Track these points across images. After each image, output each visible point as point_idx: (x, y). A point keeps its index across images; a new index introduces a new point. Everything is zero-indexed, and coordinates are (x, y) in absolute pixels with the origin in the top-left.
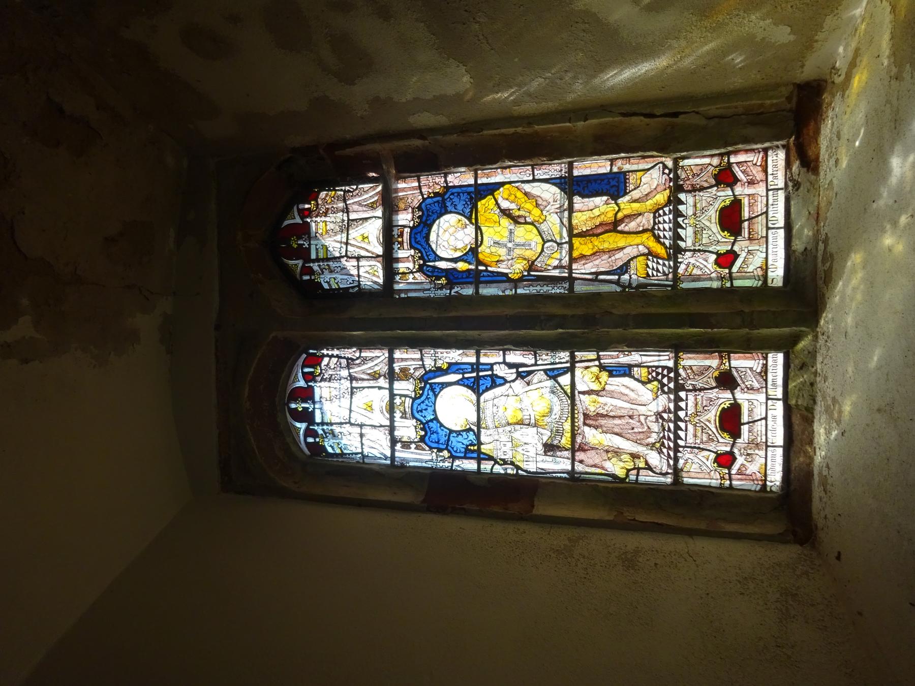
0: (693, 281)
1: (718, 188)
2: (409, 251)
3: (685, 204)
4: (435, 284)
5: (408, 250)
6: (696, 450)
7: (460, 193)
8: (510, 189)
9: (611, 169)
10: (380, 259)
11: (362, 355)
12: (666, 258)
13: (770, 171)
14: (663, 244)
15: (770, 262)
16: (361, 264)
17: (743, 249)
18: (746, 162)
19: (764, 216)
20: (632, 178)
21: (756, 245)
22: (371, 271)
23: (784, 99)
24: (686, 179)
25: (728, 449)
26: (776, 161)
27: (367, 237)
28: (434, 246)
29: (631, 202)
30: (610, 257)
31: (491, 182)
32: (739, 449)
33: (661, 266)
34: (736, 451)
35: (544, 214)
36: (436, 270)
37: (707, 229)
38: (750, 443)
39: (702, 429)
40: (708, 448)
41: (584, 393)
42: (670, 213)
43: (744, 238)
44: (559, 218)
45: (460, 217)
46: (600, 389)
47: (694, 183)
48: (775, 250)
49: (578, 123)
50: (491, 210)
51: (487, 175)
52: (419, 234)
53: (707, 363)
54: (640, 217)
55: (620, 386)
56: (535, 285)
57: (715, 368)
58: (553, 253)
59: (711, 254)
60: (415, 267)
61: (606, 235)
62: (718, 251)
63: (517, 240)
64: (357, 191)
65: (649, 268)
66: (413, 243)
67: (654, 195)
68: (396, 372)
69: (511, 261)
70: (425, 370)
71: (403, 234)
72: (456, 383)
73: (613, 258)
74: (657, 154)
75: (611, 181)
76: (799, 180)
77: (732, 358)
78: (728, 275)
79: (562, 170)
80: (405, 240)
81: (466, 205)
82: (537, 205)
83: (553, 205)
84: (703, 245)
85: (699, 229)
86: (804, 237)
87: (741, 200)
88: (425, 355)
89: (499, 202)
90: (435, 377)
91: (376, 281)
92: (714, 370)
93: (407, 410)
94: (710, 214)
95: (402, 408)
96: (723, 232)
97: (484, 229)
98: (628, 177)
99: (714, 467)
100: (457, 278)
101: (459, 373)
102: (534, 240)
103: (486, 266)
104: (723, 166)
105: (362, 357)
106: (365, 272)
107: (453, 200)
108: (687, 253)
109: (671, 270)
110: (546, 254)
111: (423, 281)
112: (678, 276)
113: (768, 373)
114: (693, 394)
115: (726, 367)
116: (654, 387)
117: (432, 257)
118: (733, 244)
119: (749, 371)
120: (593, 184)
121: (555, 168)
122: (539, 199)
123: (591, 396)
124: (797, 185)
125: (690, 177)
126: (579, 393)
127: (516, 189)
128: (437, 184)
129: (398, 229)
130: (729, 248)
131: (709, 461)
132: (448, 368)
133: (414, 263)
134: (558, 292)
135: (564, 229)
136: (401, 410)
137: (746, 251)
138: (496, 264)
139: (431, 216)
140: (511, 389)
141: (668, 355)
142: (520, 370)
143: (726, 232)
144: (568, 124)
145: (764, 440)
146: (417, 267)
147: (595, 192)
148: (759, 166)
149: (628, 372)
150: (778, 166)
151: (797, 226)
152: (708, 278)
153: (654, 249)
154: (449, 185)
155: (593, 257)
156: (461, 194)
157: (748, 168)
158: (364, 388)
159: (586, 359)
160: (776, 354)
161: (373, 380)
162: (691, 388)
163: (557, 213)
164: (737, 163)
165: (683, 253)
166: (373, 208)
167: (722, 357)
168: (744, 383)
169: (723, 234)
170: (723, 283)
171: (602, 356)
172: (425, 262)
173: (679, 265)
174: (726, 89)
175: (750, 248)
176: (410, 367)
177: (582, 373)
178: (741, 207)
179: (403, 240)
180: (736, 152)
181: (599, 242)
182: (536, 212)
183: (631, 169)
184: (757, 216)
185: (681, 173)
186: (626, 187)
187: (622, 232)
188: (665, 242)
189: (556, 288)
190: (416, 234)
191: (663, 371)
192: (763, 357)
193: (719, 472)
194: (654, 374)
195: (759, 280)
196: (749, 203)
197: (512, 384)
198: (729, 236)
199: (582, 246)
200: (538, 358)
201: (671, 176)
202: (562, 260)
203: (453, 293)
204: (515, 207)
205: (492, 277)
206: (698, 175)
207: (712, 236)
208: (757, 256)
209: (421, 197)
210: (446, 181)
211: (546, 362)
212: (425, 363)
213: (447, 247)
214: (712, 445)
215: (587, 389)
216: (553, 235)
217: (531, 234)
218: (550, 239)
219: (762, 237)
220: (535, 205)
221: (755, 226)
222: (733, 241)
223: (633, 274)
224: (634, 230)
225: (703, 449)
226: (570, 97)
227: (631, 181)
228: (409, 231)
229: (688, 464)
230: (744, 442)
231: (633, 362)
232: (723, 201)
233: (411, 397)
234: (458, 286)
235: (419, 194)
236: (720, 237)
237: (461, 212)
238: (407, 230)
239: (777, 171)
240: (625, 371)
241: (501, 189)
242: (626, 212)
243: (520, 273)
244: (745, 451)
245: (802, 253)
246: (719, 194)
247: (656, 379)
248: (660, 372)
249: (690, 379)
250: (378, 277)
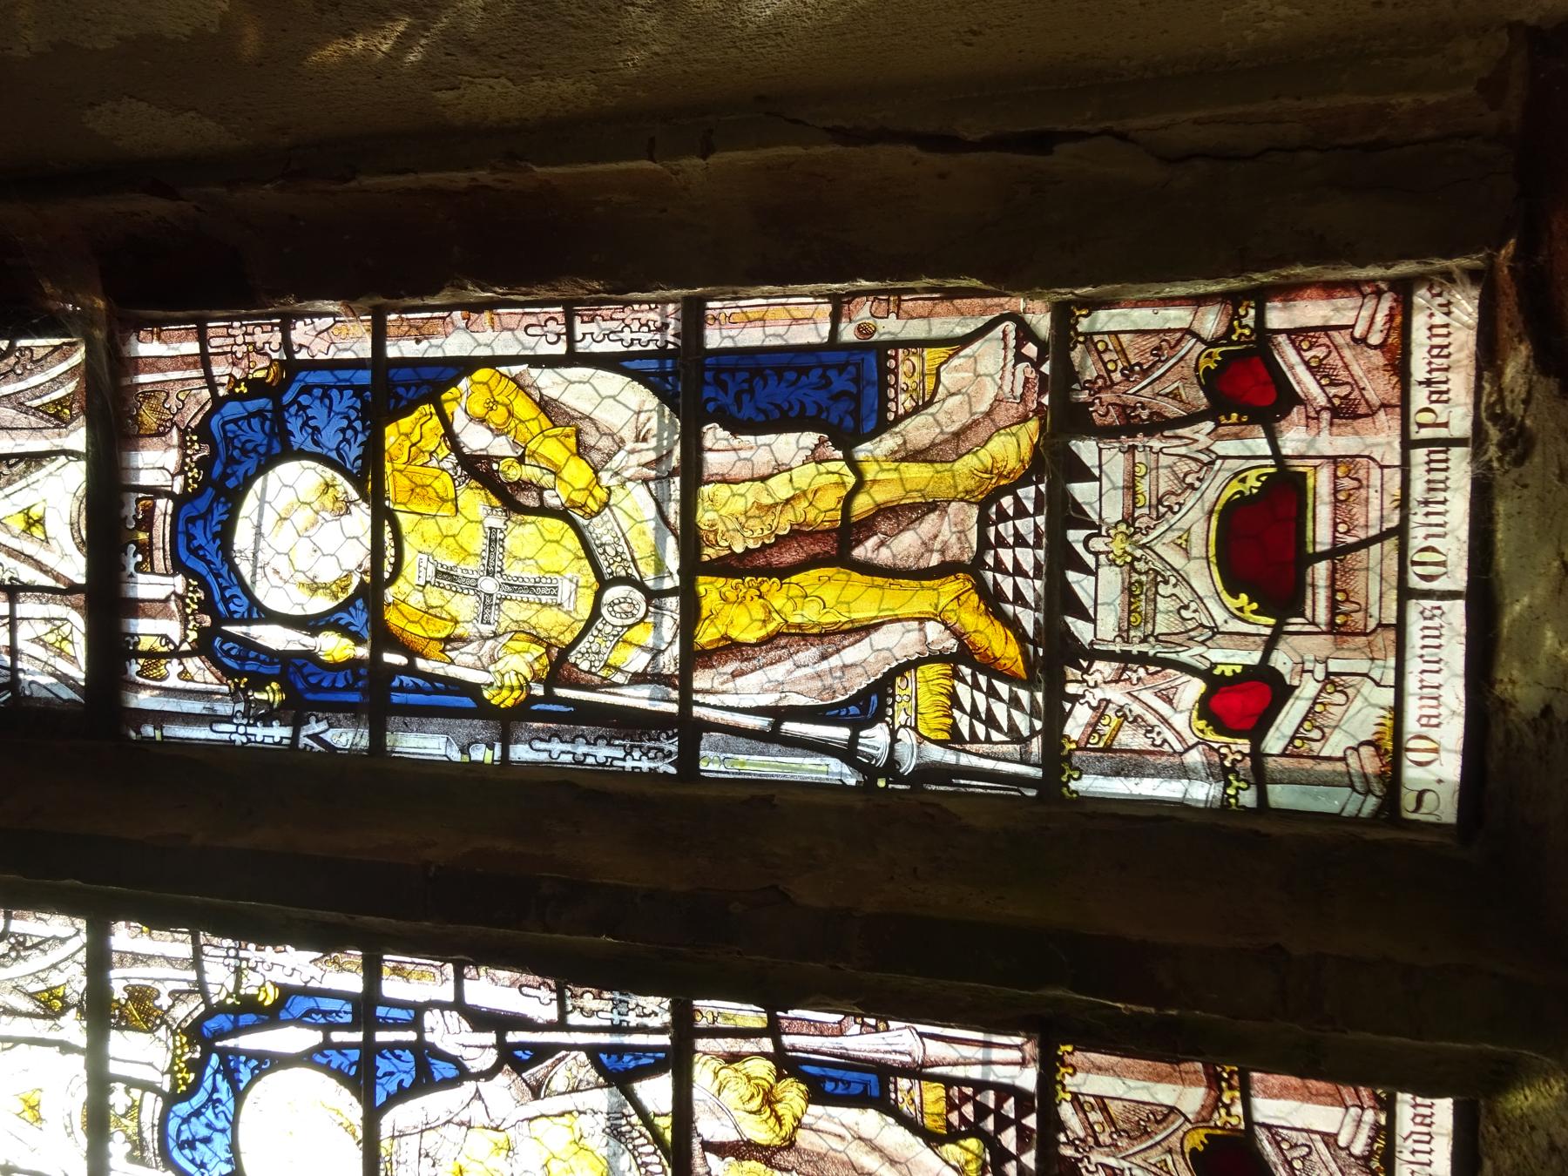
0: (1117, 774)
1: (1218, 424)
2: (169, 580)
3: (1092, 478)
4: (247, 701)
5: (167, 575)
7: (331, 387)
8: (493, 383)
9: (834, 331)
10: (80, 598)
11: (12, 929)
12: (1023, 675)
13: (1419, 370)
14: (1013, 624)
15: (1411, 725)
16: (22, 610)
17: (1308, 666)
18: (1326, 329)
19: (1391, 544)
20: (906, 367)
21: (1357, 654)
22: (51, 638)
23: (1469, 90)
24: (1100, 382)
26: (1444, 331)
27: (40, 521)
28: (245, 569)
29: (903, 460)
30: (824, 657)
31: (431, 354)
33: (1003, 707)
35: (603, 483)
36: (252, 654)
37: (1173, 580)
41: (721, 1149)
42: (1038, 511)
43: (1317, 625)
44: (656, 500)
45: (329, 473)
46: (777, 1142)
47: (1131, 400)
48: (1431, 679)
49: (684, 162)
50: (431, 454)
51: (418, 328)
52: (200, 523)
53: (1165, 1094)
54: (933, 516)
55: (849, 1137)
56: (567, 737)
57: (1190, 1117)
58: (630, 627)
59: (1188, 677)
60: (186, 636)
61: (814, 573)
62: (1214, 665)
63: (513, 570)
64: (12, 360)
65: (962, 709)
66: (184, 554)
67: (985, 435)
68: (116, 997)
69: (490, 643)
70: (206, 1000)
71: (153, 516)
72: (305, 1059)
73: (835, 661)
74: (976, 283)
75: (832, 374)
76: (1528, 422)
77: (1257, 1087)
78: (1248, 760)
79: (665, 326)
80: (158, 542)
81: (349, 433)
82: (582, 450)
83: (632, 452)
84: (1157, 640)
85: (1144, 578)
86: (1542, 659)
87: (1304, 475)
88: (206, 949)
89: (457, 428)
90: (237, 1031)
91: (66, 675)
92: (1190, 1126)
93: (147, 1135)
94: (1184, 524)
95: (132, 1127)
96: (1235, 595)
97: (405, 521)
98: (892, 363)
100: (317, 688)
101: (315, 1026)
102: (568, 574)
103: (411, 652)
104: (1238, 343)
105: (13, 935)
106: (33, 641)
107: (310, 412)
108: (1098, 665)
109: (1038, 725)
110: (608, 629)
111: (210, 687)
112: (1063, 747)
113: (1398, 1162)
115: (1234, 1121)
116: (970, 1156)
117: (240, 607)
118: (1270, 645)
119: (1321, 1146)
120: (772, 382)
121: (644, 317)
122: (586, 426)
123: (746, 1163)
124: (1518, 443)
125: (1117, 376)
126: (708, 1146)
127: (513, 385)
128: (260, 352)
129: (138, 500)
130: (1254, 658)
132: (280, 1004)
133: (185, 621)
134: (645, 769)
135: (671, 544)
136: (130, 1132)
137: (1320, 673)
138: (443, 651)
139: (240, 463)
140: (477, 1104)
141: (1019, 1047)
142: (513, 1037)
143: (1244, 597)
144: (647, 164)
146: (193, 635)
147: (777, 414)
148: (1375, 347)
149: (875, 1092)
150: (1451, 349)
151: (1517, 608)
152: (1172, 766)
153: (979, 640)
154: (298, 356)
155: (767, 652)
156: (335, 393)
157: (1334, 354)
158: (16, 1041)
159: (730, 1024)
160: (1428, 1101)
161: (44, 1017)
163: (645, 481)
164: (1296, 334)
165: (1085, 664)
166: (62, 420)
167: (1219, 1078)
169: (1232, 603)
170: (1231, 791)
171: (785, 1023)
172: (218, 620)
173: (1068, 706)
174: (1229, 45)
175: (1334, 666)
176: (158, 986)
177: (716, 1074)
178: (1306, 505)
179: (151, 537)
180: (1289, 291)
181: (789, 598)
182: (577, 473)
183: (903, 336)
184: (1366, 543)
185: (1083, 359)
186: (884, 400)
187: (868, 569)
188: (1020, 616)
189: (637, 754)
190: (191, 520)
191: (1000, 1102)
192: (1377, 1098)
194: (968, 1110)
195: (1368, 792)
196: (1336, 492)
197: (483, 1085)
198: (1254, 612)
199: (727, 607)
200: (569, 1002)
201: (1046, 368)
202: (660, 652)
203: (304, 741)
204: (507, 451)
205: (428, 693)
206: (1145, 373)
207: (1193, 606)
208: (1359, 698)
209: (206, 394)
210: (286, 344)
211: (593, 1021)
212: (208, 978)
213: (286, 575)
215: (732, 1136)
216: (634, 560)
217: (559, 548)
218: (623, 573)
219: (1380, 625)
220: (575, 451)
221: (1357, 583)
222: (1268, 631)
223: (905, 726)
224: (911, 563)
226: (634, 59)
227: (902, 379)
228: (170, 511)
231: (893, 1056)
232: (1236, 474)
233: (158, 1092)
234: (320, 715)
235: (202, 383)
236: (1220, 615)
237: (334, 455)
238: (164, 505)
239: (1446, 370)
240: (866, 1084)
241: (464, 384)
242: (882, 495)
243: (521, 687)
245: (1534, 724)
246: (1222, 447)
247: (975, 1130)
248: (992, 1105)
249: (1098, 1143)
250: (73, 660)
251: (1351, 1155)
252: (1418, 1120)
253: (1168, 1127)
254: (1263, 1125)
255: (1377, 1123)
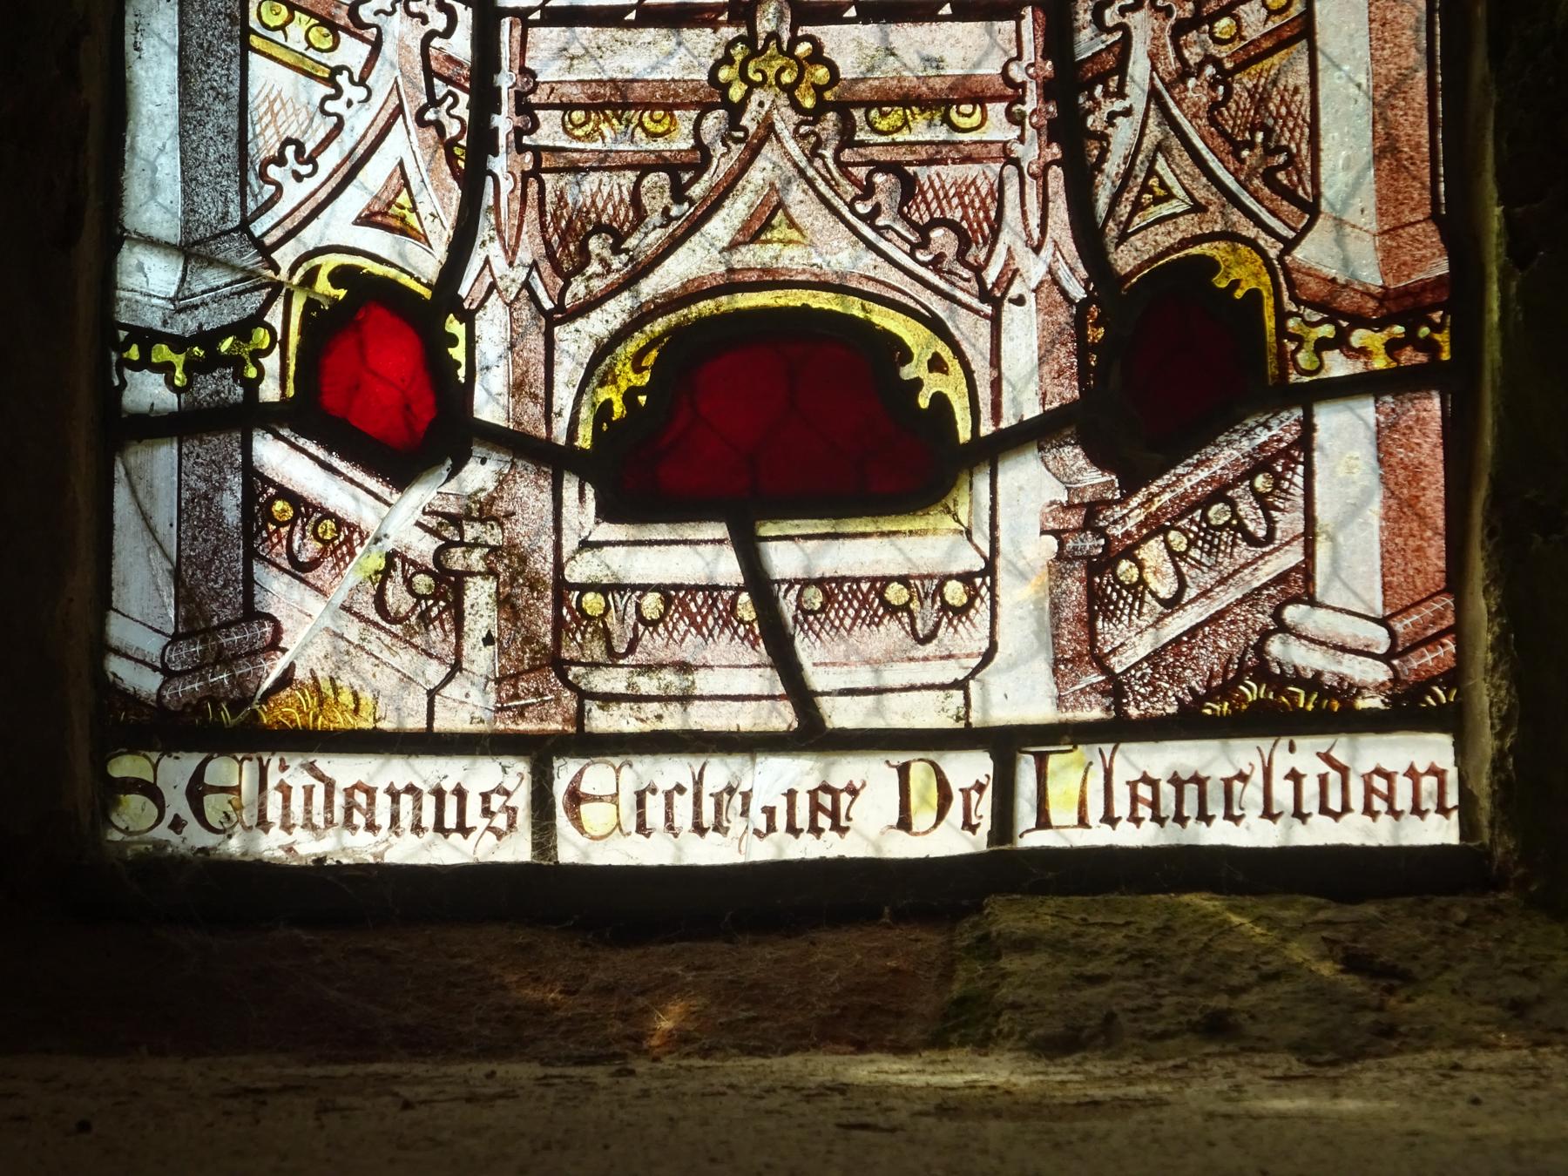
6: (462, 110)
25: (490, 406)
32: (501, 507)
34: (479, 475)
38: (559, 601)
39: (675, 168)
40: (485, 230)
57: (1299, 253)
92: (1273, 253)
99: (310, 278)
113: (1266, 744)
114: (1030, 67)
115: (1304, 359)
131: (375, 240)
145: (601, 721)
162: (1087, 42)
168: (1155, 527)
192: (1423, 686)
193: (257, 319)
214: (525, 255)
225: (472, 178)
229: (321, 37)
230: (570, 543)
244: (476, 560)
249: (1180, 29)
251: (1265, 634)
252: (1380, 784)
253: (1259, 201)
254: (1308, 427)
255: (1359, 690)
